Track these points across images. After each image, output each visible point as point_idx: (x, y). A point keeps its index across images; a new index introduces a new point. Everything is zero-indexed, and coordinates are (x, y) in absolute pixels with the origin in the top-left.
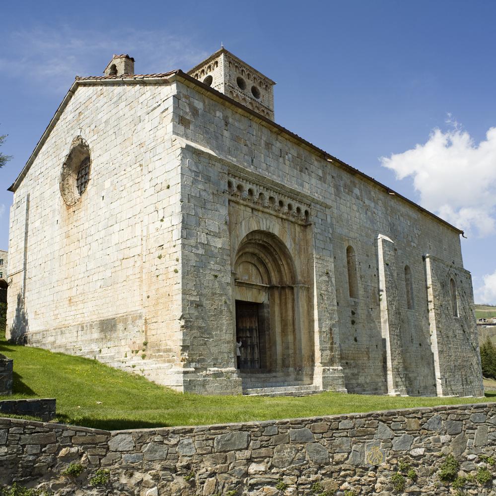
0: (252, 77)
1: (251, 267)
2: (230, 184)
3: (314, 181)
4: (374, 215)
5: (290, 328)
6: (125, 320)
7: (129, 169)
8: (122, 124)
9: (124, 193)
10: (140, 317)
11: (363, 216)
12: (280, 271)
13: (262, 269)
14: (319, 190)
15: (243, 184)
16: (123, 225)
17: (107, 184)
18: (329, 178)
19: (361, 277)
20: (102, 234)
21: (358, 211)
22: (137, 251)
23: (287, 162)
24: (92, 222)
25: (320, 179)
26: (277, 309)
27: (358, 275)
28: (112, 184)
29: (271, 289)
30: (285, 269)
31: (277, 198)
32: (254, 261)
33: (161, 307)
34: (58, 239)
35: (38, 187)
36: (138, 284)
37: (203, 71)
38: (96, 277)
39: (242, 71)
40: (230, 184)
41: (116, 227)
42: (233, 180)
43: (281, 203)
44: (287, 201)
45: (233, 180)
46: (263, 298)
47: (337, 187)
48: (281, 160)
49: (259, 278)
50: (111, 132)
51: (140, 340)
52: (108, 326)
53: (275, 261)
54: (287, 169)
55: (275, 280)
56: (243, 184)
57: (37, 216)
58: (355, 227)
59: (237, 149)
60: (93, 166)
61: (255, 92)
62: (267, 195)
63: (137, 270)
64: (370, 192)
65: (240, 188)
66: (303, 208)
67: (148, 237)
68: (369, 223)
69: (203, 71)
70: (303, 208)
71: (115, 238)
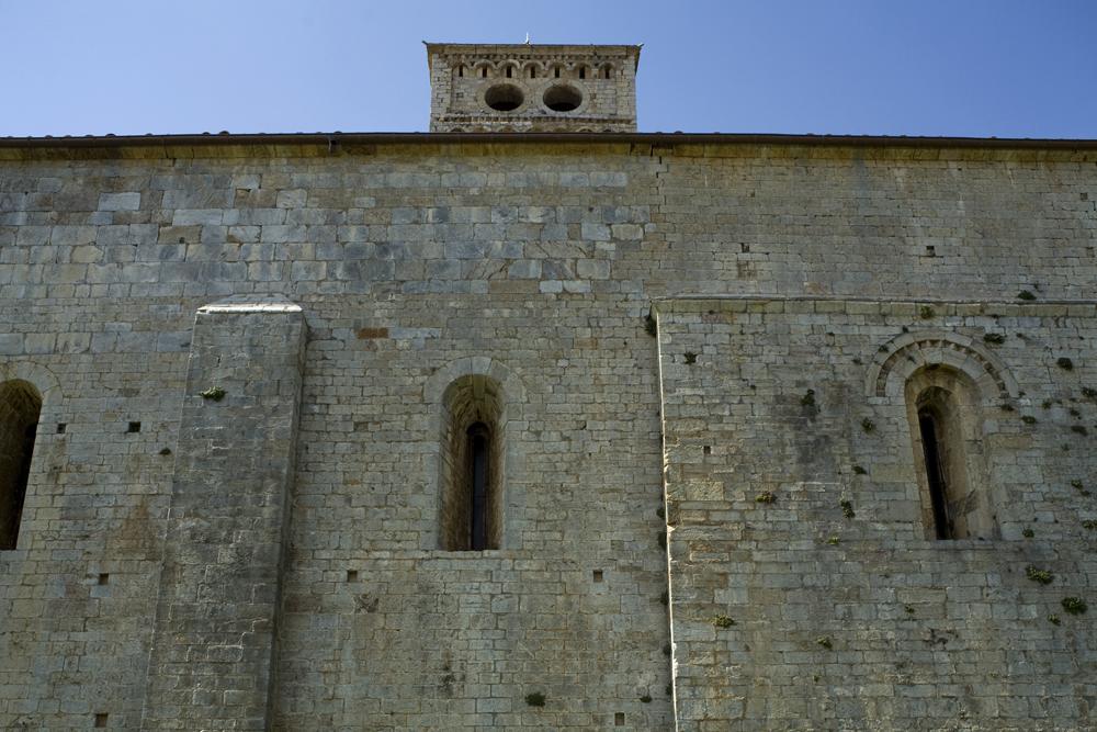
4: (226, 247)
64: (221, 183)
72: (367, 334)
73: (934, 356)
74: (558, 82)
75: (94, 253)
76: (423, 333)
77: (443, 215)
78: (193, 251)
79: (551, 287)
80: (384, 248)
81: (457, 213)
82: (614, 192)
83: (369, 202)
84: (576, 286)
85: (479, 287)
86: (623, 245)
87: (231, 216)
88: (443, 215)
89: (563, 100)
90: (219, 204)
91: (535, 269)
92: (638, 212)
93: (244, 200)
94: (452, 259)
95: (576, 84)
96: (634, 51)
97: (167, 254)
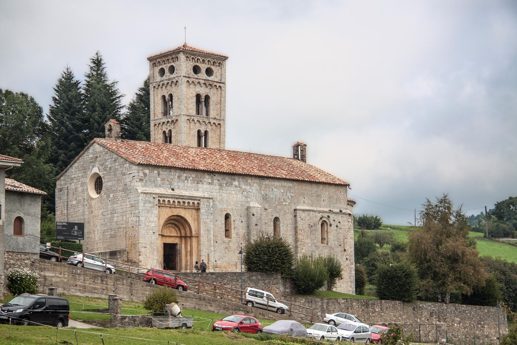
0: (206, 62)
1: (171, 228)
2: (159, 200)
3: (205, 186)
5: (189, 254)
6: (120, 252)
7: (120, 193)
8: (117, 172)
9: (119, 202)
10: (126, 251)
11: (240, 196)
12: (185, 230)
13: (177, 229)
14: (208, 190)
15: (165, 199)
16: (119, 215)
17: (111, 196)
18: (216, 182)
19: (234, 228)
20: (110, 216)
21: (236, 194)
22: (125, 226)
23: (189, 182)
24: (105, 210)
25: (210, 183)
26: (183, 246)
27: (232, 227)
28: (113, 196)
29: (181, 237)
30: (188, 229)
31: (181, 201)
32: (173, 226)
33: (133, 248)
34: (87, 213)
35: (74, 184)
36: (124, 238)
37: (168, 60)
38: (107, 234)
39: (198, 59)
40: (159, 200)
41: (116, 215)
42: (160, 199)
43: (184, 202)
44: (187, 201)
45: (160, 199)
46: (176, 241)
47: (221, 185)
48: (186, 181)
49: (175, 232)
50: (112, 173)
51: (126, 259)
52: (113, 254)
53: (183, 225)
54: (189, 185)
55: (183, 235)
56: (165, 199)
57: (74, 199)
58: (232, 203)
59: (164, 184)
60: (104, 185)
61: (209, 72)
62: (176, 201)
63: (124, 233)
64: (247, 181)
65: (164, 201)
66: (196, 202)
67: (128, 222)
68: (244, 198)
69: (168, 60)
70: (196, 202)
71: (115, 219)
72: (266, 209)
73: (324, 219)
74: (209, 66)
75: (233, 192)
76: (271, 209)
77: (272, 190)
78: (245, 193)
79: (284, 203)
80: (266, 195)
81: (274, 189)
82: (291, 187)
83: (264, 186)
84: (287, 203)
85: (277, 203)
86: (292, 197)
87: (249, 187)
88: (272, 190)
89: (209, 72)
90: (247, 185)
91: (282, 201)
92: (293, 191)
93: (250, 185)
94: (274, 197)
95: (213, 68)
96: (225, 58)
97: (242, 194)
